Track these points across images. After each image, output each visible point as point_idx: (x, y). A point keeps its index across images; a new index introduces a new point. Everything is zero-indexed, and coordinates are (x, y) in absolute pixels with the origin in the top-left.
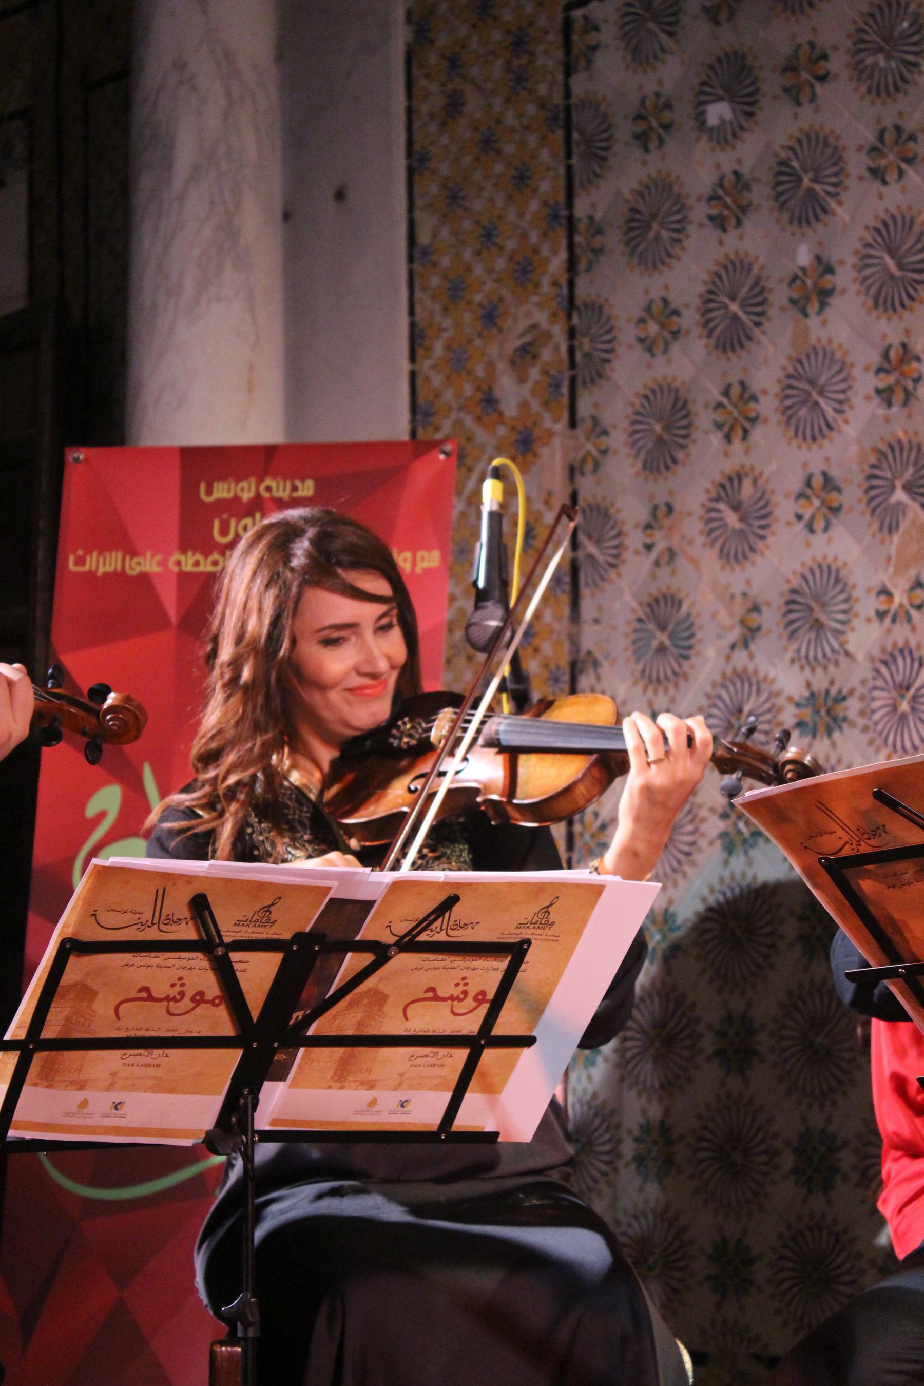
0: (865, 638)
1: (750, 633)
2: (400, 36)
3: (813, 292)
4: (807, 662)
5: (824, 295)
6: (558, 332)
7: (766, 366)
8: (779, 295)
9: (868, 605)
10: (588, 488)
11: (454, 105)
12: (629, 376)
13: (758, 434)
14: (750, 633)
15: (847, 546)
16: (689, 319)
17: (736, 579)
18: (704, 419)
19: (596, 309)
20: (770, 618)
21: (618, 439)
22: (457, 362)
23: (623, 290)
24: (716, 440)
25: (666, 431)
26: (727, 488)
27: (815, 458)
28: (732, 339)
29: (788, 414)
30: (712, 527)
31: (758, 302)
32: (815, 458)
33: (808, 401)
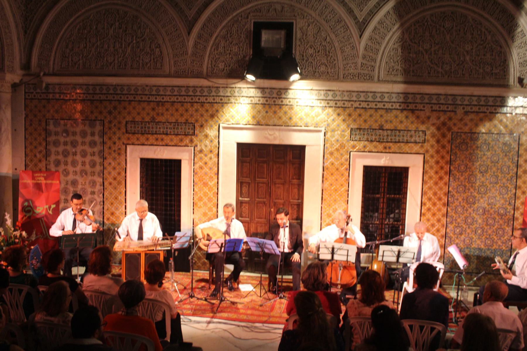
0: (80, 187)
1: (67, 184)
2: (24, 116)
3: (75, 154)
4: (73, 187)
5: (76, 155)
6: (45, 151)
7: (70, 159)
8: (71, 153)
9: (80, 183)
10: (48, 167)
11: (31, 125)
12: (53, 158)
13: (68, 166)
14: (67, 184)
15: (78, 177)
16: (61, 153)
17: (66, 179)
18: (62, 163)
19: (49, 150)
20: (69, 183)
21: (52, 163)
22: (31, 151)
23: (53, 149)
24: (63, 165)
25: (58, 163)
26: (65, 170)
27: (75, 169)
28: (65, 156)
29: (72, 165)
30: (63, 173)
31: (69, 153)
32: (75, 169)
33: (74, 164)
